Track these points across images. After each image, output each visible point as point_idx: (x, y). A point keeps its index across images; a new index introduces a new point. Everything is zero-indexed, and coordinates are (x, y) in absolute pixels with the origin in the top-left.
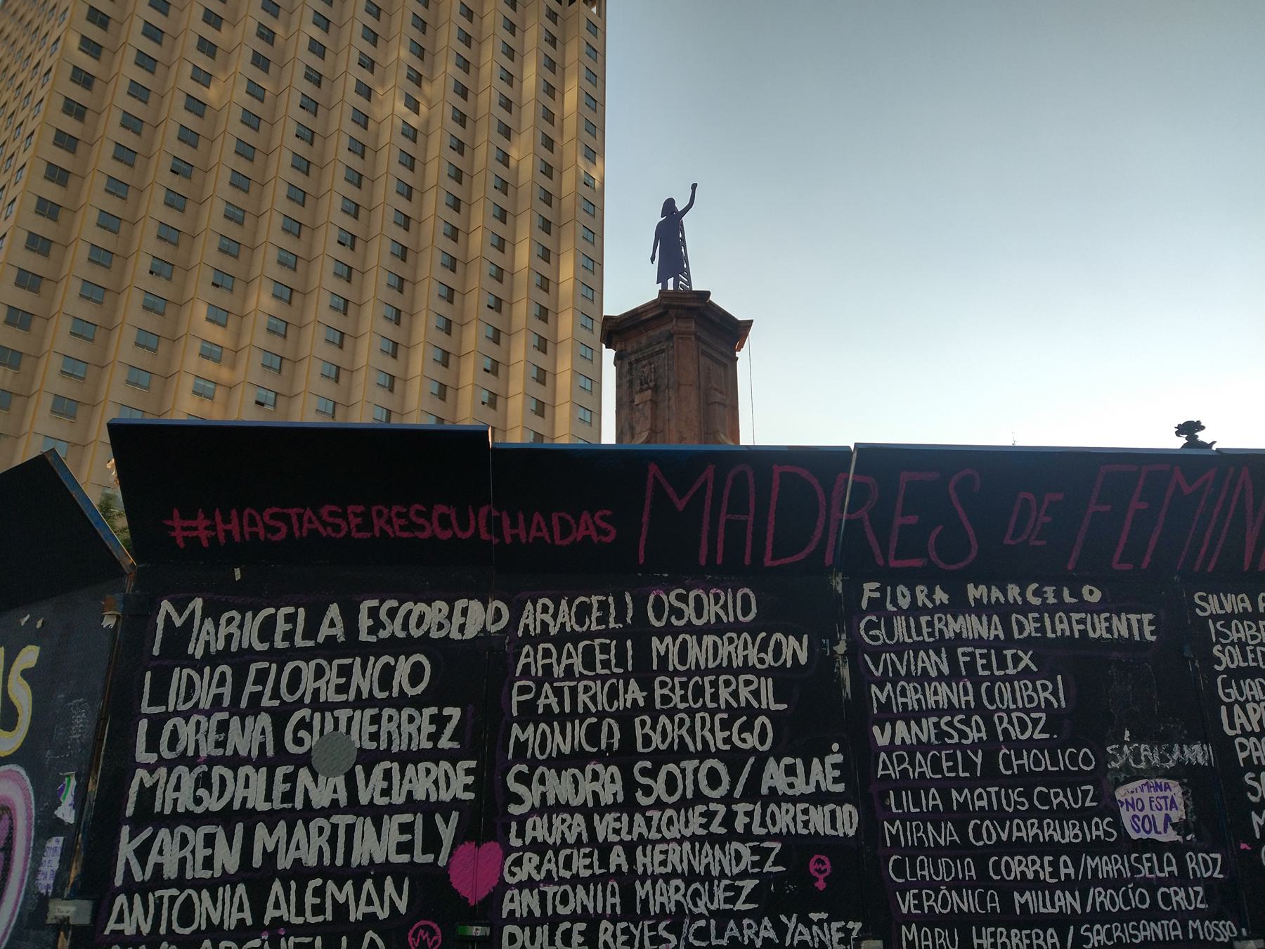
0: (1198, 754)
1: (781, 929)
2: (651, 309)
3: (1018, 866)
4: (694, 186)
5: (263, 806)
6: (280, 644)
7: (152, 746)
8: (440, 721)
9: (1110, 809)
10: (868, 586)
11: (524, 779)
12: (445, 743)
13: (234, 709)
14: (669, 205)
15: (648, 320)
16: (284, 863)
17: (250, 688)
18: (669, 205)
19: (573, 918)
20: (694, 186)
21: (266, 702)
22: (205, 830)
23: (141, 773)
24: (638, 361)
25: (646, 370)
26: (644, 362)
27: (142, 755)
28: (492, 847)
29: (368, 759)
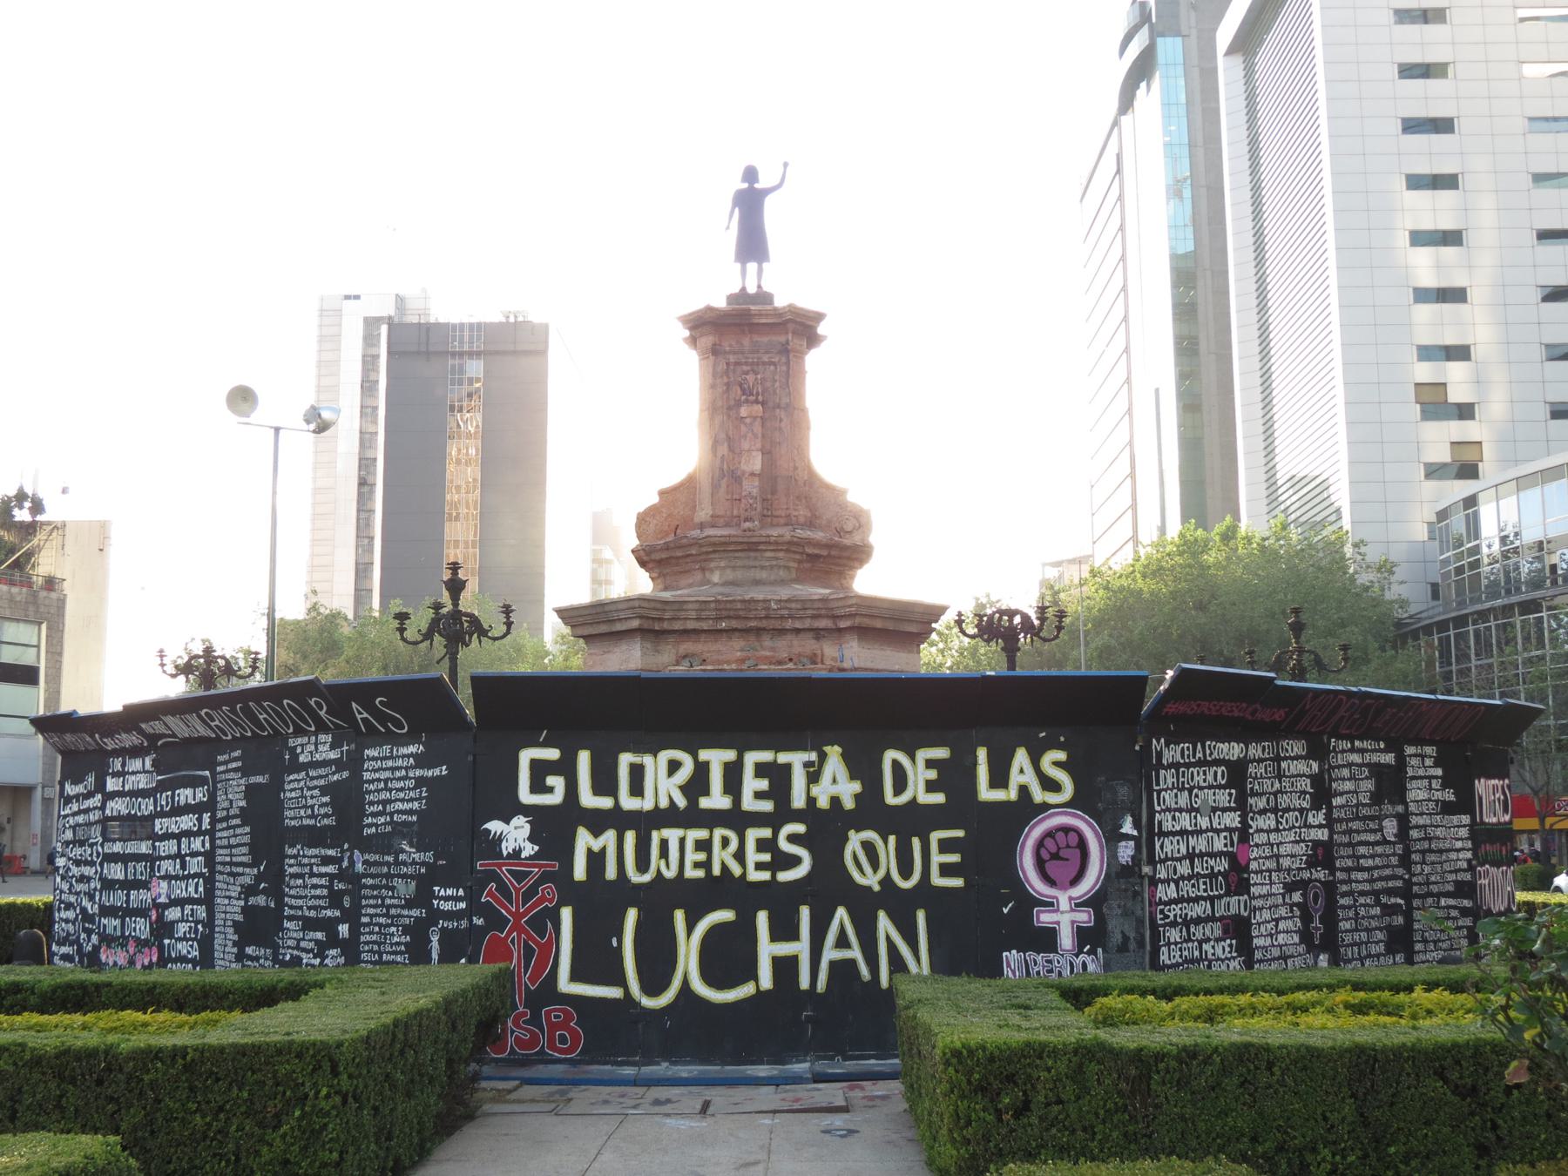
0: (1400, 808)
1: (1311, 873)
2: (767, 315)
3: (1362, 850)
4: (786, 165)
5: (1190, 829)
6: (1187, 761)
7: (1159, 804)
8: (1230, 795)
9: (1381, 829)
10: (1333, 740)
11: (1252, 819)
12: (1233, 805)
13: (1179, 790)
14: (750, 174)
15: (758, 324)
16: (1197, 851)
17: (1181, 780)
18: (750, 174)
19: (1266, 871)
20: (786, 165)
21: (1187, 786)
22: (1177, 838)
23: (1157, 815)
24: (737, 364)
25: (750, 378)
26: (745, 368)
27: (1157, 808)
28: (1246, 845)
29: (1214, 810)
